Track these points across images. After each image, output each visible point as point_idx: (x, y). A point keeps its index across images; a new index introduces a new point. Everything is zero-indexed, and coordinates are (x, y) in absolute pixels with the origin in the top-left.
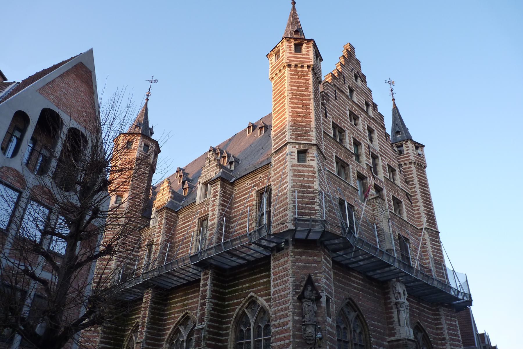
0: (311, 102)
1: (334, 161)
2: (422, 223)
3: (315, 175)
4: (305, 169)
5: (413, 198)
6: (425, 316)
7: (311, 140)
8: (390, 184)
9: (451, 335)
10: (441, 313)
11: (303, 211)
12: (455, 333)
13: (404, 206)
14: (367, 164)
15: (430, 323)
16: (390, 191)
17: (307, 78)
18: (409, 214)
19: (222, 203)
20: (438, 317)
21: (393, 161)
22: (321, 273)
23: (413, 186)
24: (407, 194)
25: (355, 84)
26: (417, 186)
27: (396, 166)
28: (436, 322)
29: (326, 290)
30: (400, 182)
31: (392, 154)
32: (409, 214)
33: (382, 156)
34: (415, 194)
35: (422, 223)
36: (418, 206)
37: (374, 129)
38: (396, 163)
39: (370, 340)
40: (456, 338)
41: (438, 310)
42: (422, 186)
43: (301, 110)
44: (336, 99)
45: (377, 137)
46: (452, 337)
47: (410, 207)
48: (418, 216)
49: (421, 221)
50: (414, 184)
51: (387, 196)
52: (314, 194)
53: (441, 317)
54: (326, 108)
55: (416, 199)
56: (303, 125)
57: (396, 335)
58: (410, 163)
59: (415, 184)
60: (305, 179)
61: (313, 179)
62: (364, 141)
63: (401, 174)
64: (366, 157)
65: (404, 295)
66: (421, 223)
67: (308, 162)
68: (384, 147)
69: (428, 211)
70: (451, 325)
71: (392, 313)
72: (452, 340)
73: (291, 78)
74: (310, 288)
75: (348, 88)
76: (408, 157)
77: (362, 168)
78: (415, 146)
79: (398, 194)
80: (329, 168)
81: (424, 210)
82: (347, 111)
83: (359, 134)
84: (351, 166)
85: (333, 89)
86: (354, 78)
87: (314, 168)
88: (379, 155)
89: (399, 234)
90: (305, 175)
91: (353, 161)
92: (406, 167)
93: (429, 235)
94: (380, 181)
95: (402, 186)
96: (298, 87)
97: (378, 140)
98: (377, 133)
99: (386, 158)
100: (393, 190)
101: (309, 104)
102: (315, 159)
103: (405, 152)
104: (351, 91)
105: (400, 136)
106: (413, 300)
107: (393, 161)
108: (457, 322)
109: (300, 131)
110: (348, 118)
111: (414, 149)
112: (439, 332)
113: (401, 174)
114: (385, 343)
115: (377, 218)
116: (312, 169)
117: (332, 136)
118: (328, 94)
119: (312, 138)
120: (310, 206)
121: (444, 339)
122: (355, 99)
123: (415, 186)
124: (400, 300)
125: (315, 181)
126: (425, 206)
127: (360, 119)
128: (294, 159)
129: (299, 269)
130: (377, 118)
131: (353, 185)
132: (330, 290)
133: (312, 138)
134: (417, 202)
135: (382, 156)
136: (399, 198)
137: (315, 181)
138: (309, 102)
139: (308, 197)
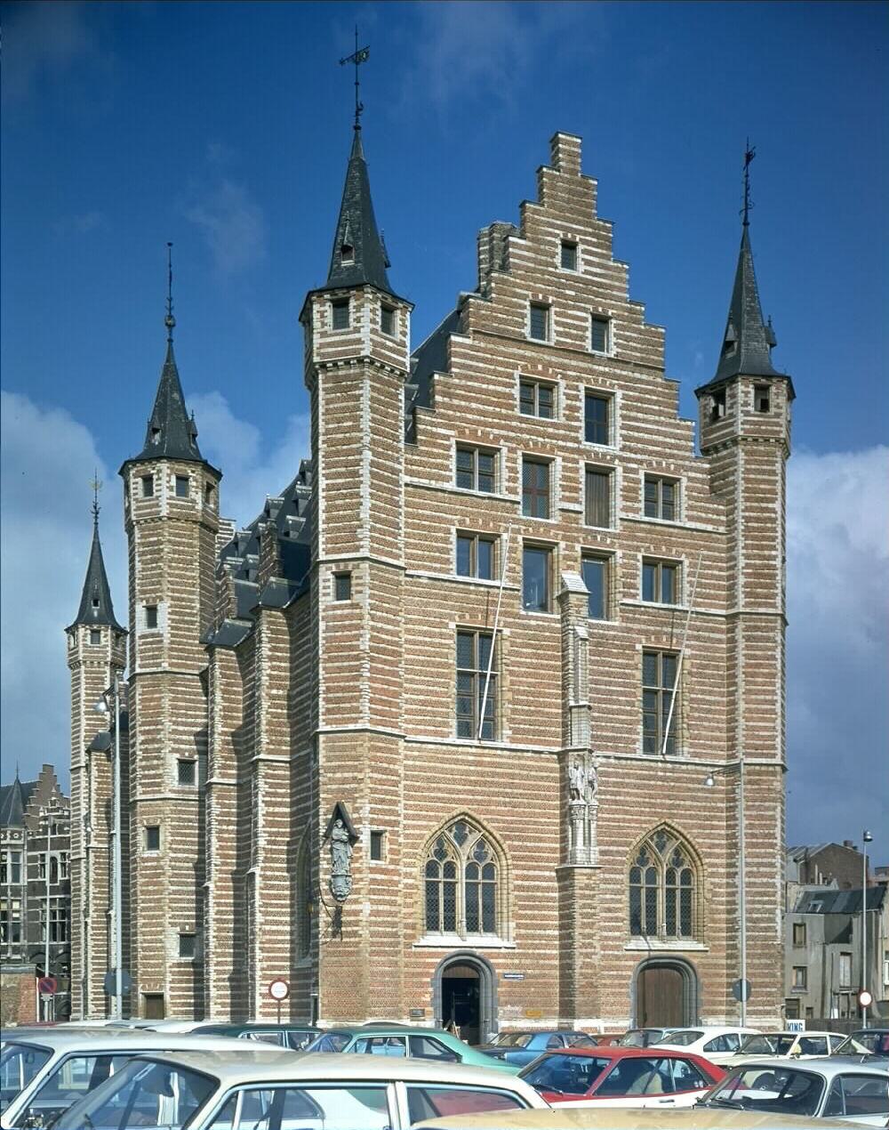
11: (340, 695)
19: (270, 653)
22: (362, 797)
74: (340, 823)
101: (357, 463)
116: (358, 611)
119: (362, 543)
133: (362, 543)
139: (350, 669)
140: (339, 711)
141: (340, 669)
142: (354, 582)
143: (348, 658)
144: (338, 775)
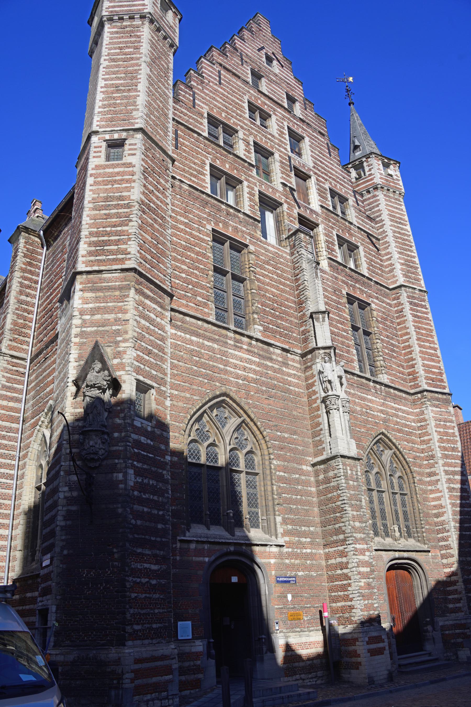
0: (141, 68)
1: (208, 173)
2: (397, 278)
3: (135, 177)
4: (117, 170)
5: (381, 242)
6: (397, 423)
7: (133, 124)
8: (332, 218)
9: (445, 449)
10: (427, 417)
11: (106, 238)
12: (452, 446)
13: (362, 253)
14: (283, 183)
15: (410, 434)
16: (332, 228)
17: (138, 34)
18: (372, 265)
19: (24, 266)
20: (422, 424)
21: (341, 184)
22: (125, 341)
23: (381, 224)
24: (369, 235)
25: (269, 69)
26: (388, 223)
27: (349, 193)
28: (420, 432)
29: (138, 371)
30: (356, 217)
31: (341, 175)
32: (372, 265)
33: (319, 176)
34: (384, 235)
35: (397, 278)
36: (389, 253)
37: (305, 135)
38: (348, 189)
39: (270, 463)
40: (454, 453)
41: (422, 413)
42: (396, 222)
43: (122, 82)
44: (220, 83)
45: (309, 148)
46: (446, 453)
47: (374, 256)
48: (390, 268)
49: (394, 276)
50: (382, 221)
51: (326, 235)
52: (129, 208)
53: (428, 422)
54: (194, 93)
55: (387, 242)
56: (121, 104)
57: (324, 453)
58: (376, 188)
59: (384, 220)
60: (116, 186)
61: (129, 185)
62: (279, 150)
63: (358, 204)
64: (282, 173)
65: (342, 384)
66: (395, 279)
67: (124, 158)
68: (323, 163)
69: (407, 260)
70: (446, 434)
71: (319, 416)
72: (446, 457)
73: (111, 38)
75: (249, 72)
76: (372, 179)
77: (273, 188)
78: (382, 163)
79: (351, 235)
80: (194, 182)
81: (400, 258)
82: (244, 102)
83: (269, 139)
84: (245, 183)
85: (214, 69)
86: (264, 59)
87: (134, 166)
88: (311, 173)
89: (348, 294)
90: (115, 181)
91: (252, 177)
92: (369, 196)
93: (408, 297)
94: (312, 211)
95: (358, 223)
96: (120, 48)
97: (312, 152)
98: (310, 141)
99: (326, 180)
100: (339, 227)
101: (137, 71)
102: (138, 153)
103: (367, 174)
104: (257, 76)
105: (361, 152)
106: (374, 398)
107: (341, 184)
108: (456, 429)
109: (115, 112)
110: (245, 113)
111: (381, 167)
112: (425, 446)
113: (358, 204)
114: (304, 467)
115: (296, 265)
116: (131, 169)
117: (206, 134)
118: (203, 75)
119: (136, 121)
120: (119, 228)
121: (433, 457)
122: (264, 89)
123: (384, 223)
124: (330, 393)
125: (133, 188)
126: (400, 253)
127: (274, 118)
128: (99, 157)
129: (86, 338)
130: (310, 121)
131: (248, 212)
132: (154, 373)
133: (136, 121)
134: (387, 248)
135: (319, 176)
136: (353, 240)
137: (133, 188)
138: (138, 68)
139: (118, 215)
140: (103, 252)
141: (108, 216)
142: (126, 147)
143: (117, 206)
144: (98, 317)
